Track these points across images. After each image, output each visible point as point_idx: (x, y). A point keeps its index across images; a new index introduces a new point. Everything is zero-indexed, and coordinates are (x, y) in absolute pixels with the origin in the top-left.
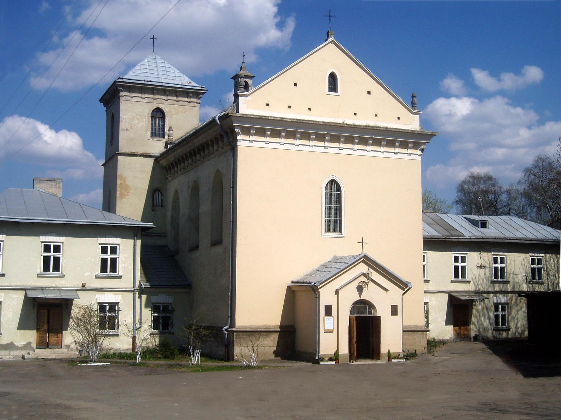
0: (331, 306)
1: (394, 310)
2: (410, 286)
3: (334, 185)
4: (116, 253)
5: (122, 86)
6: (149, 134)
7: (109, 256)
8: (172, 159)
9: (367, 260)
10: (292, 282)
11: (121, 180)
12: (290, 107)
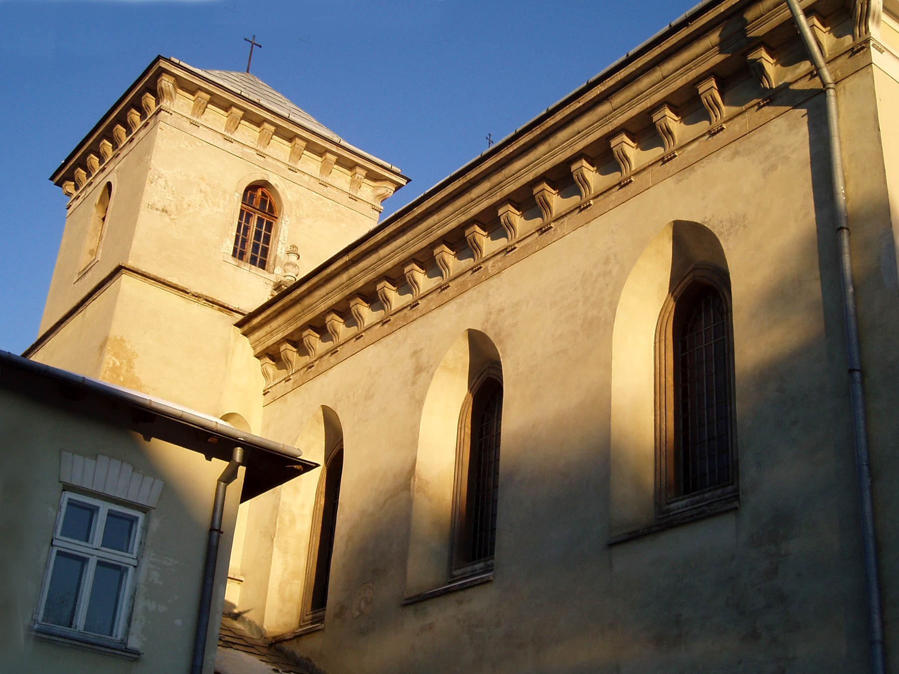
4: (124, 546)
6: (230, 245)
7: (94, 549)
8: (336, 298)
11: (116, 355)
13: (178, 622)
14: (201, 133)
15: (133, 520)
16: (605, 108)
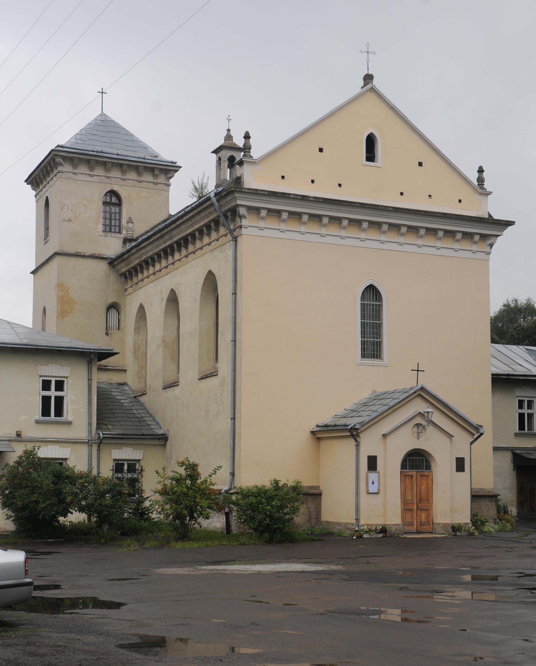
0: (375, 457)
1: (460, 465)
2: (481, 431)
3: (372, 293)
5: (63, 158)
6: (101, 227)
7: (53, 393)
8: (137, 261)
9: (422, 393)
10: (317, 426)
12: (313, 181)
13: (83, 410)
14: (80, 177)
15: (63, 381)
16: (190, 223)
